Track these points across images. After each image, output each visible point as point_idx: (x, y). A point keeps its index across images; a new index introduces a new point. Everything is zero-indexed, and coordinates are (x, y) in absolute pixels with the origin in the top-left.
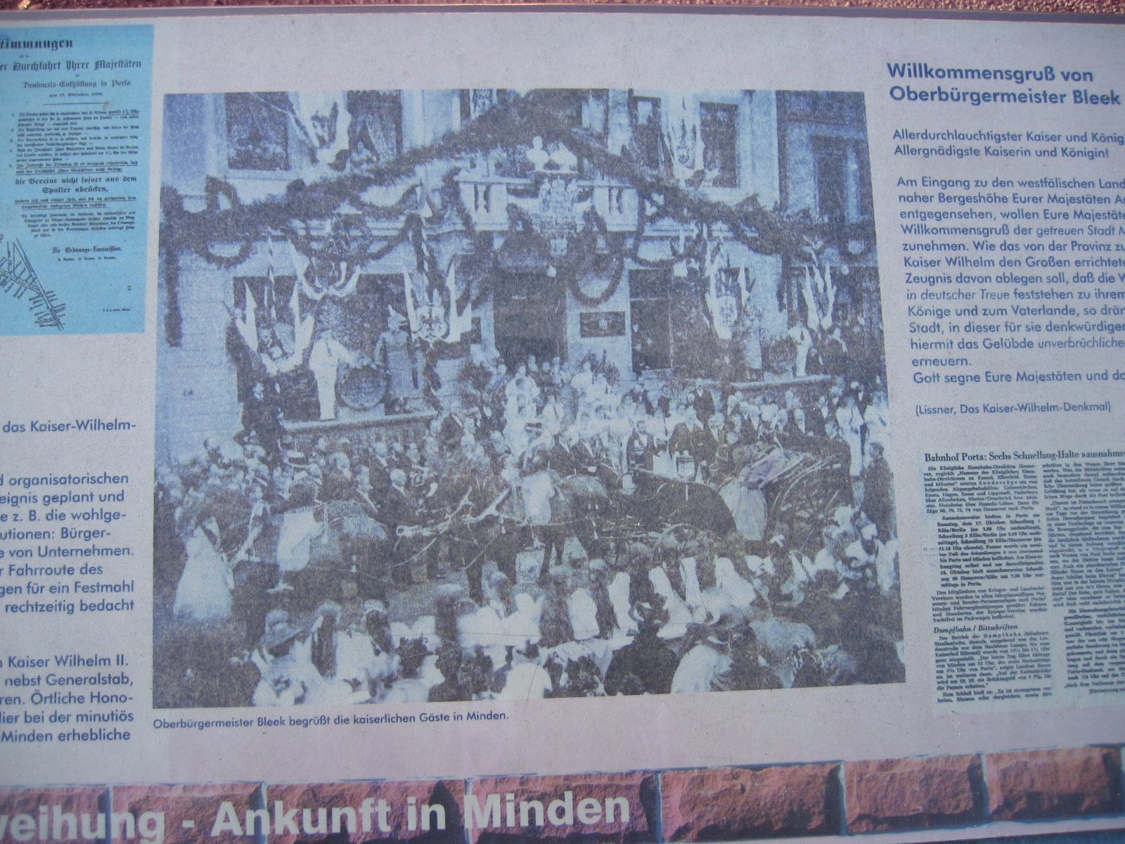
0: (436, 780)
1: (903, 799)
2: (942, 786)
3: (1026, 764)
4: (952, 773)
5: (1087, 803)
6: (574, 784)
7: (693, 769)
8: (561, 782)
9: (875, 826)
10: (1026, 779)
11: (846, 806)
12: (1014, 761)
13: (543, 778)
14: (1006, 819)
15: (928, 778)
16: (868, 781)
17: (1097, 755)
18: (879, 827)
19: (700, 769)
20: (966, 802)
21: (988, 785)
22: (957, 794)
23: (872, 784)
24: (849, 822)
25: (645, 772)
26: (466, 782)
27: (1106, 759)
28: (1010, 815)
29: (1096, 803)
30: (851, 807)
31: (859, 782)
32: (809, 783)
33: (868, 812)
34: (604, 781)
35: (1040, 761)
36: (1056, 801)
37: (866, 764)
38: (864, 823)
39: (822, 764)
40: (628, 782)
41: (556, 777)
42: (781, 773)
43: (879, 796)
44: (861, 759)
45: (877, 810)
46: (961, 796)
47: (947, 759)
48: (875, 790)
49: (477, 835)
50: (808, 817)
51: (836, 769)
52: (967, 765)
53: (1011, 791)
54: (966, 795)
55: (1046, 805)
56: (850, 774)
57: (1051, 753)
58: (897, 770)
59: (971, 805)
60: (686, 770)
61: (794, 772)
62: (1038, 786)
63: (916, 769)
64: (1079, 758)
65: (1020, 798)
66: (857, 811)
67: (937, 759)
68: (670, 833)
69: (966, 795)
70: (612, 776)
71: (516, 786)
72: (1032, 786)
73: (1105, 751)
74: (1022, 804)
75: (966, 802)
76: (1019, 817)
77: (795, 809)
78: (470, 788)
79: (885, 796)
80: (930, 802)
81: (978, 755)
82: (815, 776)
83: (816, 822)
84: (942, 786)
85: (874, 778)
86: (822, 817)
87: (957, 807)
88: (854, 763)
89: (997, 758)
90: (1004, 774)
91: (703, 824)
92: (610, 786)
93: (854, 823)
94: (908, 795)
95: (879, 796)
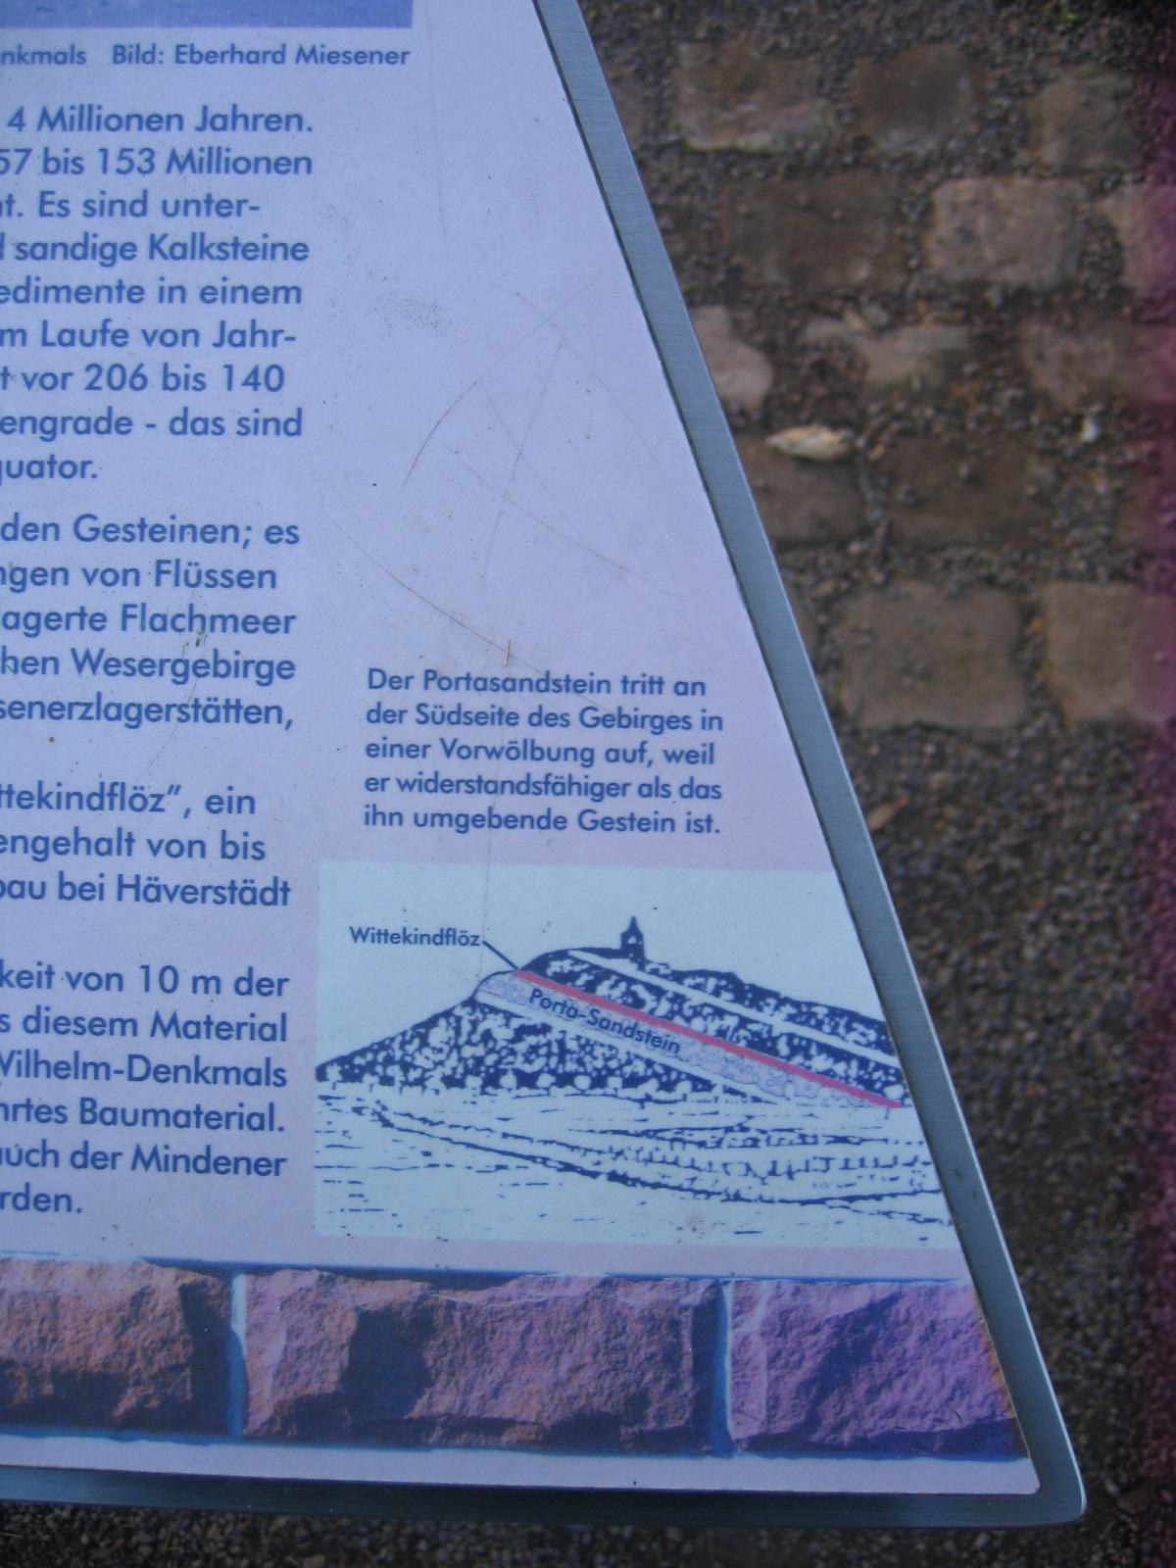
5: (128, 1401)
17: (167, 1286)
27: (189, 1296)
29: (154, 1403)
36: (48, 1388)
55: (22, 1393)
57: (45, 1268)
64: (122, 1288)
73: (190, 1278)
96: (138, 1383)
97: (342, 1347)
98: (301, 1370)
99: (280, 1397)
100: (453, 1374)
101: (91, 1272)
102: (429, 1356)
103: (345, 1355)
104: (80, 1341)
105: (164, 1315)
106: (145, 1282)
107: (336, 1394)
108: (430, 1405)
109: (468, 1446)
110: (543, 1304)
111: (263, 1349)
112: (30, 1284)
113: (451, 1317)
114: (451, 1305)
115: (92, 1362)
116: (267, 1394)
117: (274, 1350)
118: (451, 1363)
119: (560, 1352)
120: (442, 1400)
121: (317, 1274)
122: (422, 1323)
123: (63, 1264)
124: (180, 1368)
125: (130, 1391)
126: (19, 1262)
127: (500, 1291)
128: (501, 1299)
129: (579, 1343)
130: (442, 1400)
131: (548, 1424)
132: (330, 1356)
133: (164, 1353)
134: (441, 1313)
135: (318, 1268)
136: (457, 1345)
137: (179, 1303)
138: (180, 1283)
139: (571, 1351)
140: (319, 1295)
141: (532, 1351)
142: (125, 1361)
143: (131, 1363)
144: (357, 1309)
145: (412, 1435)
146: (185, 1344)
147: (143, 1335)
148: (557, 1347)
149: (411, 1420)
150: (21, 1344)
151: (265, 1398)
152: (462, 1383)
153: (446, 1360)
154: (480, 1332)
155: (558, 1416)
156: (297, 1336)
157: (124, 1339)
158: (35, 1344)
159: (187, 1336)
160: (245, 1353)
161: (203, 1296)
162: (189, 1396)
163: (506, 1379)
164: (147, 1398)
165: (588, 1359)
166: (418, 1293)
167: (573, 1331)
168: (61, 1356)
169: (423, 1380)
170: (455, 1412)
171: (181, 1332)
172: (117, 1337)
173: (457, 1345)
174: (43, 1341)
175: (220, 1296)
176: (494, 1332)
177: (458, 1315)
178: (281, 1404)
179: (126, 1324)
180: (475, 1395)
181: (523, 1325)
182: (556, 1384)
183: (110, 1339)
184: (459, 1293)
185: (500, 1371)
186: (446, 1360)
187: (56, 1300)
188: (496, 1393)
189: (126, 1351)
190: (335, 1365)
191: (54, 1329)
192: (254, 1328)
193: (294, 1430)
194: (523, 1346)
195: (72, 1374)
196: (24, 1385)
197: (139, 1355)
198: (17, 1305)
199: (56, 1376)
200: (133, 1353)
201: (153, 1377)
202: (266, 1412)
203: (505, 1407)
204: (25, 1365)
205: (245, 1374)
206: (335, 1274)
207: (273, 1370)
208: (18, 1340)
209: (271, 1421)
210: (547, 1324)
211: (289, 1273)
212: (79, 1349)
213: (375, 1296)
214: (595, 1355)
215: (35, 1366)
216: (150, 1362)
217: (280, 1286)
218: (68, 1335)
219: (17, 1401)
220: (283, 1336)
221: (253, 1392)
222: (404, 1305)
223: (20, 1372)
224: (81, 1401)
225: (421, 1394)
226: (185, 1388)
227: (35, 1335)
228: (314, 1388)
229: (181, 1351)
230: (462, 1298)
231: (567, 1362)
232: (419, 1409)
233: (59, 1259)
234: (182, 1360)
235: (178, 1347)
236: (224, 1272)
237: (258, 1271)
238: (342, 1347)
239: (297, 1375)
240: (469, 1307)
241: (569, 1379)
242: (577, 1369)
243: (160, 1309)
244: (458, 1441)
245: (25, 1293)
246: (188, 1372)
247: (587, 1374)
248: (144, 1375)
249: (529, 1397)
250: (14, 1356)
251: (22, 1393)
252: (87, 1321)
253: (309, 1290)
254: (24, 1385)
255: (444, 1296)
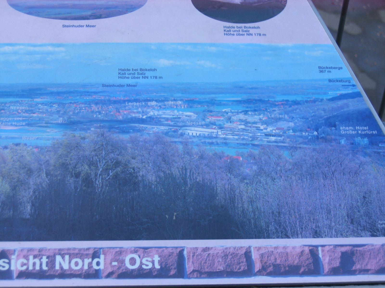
0: (2, 249)
1: (214, 264)
2: (233, 260)
3: (272, 252)
4: (237, 254)
5: (302, 270)
6: (63, 252)
7: (117, 248)
8: (57, 251)
9: (200, 275)
10: (272, 258)
11: (187, 266)
12: (267, 250)
13: (49, 250)
14: (263, 275)
15: (226, 256)
16: (197, 256)
17: (307, 249)
18: (203, 276)
19: (120, 248)
20: (243, 267)
21: (254, 260)
22: (240, 263)
23: (199, 257)
24: (188, 273)
25: (95, 248)
26: (15, 251)
27: (311, 251)
28: (265, 273)
29: (307, 270)
30: (189, 267)
31: (193, 256)
32: (170, 256)
33: (197, 269)
34: (76, 251)
35: (279, 251)
36: (287, 269)
37: (197, 248)
38: (195, 274)
39: (177, 248)
40: (87, 252)
41: (55, 249)
42: (157, 251)
43: (203, 262)
44: (195, 246)
45: (201, 268)
46: (240, 265)
47: (235, 248)
48: (201, 260)
49: (18, 273)
50: (169, 270)
51: (183, 250)
52: (244, 251)
53: (266, 263)
54: (244, 264)
55: (283, 270)
56: (189, 253)
57: (284, 248)
58: (211, 252)
59: (246, 268)
60: (114, 248)
61: (163, 251)
62: (278, 262)
63: (220, 252)
64: (299, 250)
65: (270, 266)
66: (192, 269)
67: (230, 248)
68: (105, 274)
69: (244, 264)
70: (80, 250)
71: (36, 253)
72: (276, 261)
73: (311, 248)
74: (271, 269)
75: (243, 267)
76: (270, 274)
77: (163, 266)
78: (16, 253)
79: (205, 263)
80: (227, 265)
81: (250, 247)
82: (173, 253)
83: (172, 272)
84: (233, 260)
85: (200, 254)
86: (176, 270)
87: (240, 268)
88: (191, 248)
89: (259, 249)
90: (262, 256)
91: (120, 271)
92: (79, 254)
93: (190, 273)
94: (216, 261)
95: (203, 262)
96: (303, 267)
97: (339, 258)
98: (332, 263)
99: (329, 267)
100: (359, 262)
101: (293, 248)
102: (354, 259)
103: (340, 260)
104: (292, 260)
105: (307, 254)
106: (303, 249)
107: (339, 267)
108: (355, 267)
109: (363, 274)
110: (372, 249)
111: (325, 260)
112: (282, 250)
113: (357, 252)
114: (357, 250)
115: (295, 263)
116: (327, 267)
117: (327, 259)
118: (358, 260)
119: (377, 257)
120: (357, 266)
121: (333, 246)
122: (352, 253)
123: (288, 247)
124: (310, 264)
125: (302, 268)
126: (280, 247)
127: (365, 247)
128: (365, 249)
129: (379, 255)
130: (357, 266)
131: (376, 270)
132: (337, 260)
133: (308, 261)
134: (355, 251)
135: (334, 245)
136: (359, 257)
137: (309, 252)
138: (309, 249)
139: (378, 257)
140: (334, 249)
141: (372, 257)
142: (301, 263)
143: (302, 263)
144: (341, 252)
145: (353, 273)
146: (311, 259)
147: (304, 258)
148: (376, 256)
149: (352, 270)
150: (282, 261)
151: (326, 268)
152: (360, 263)
153: (357, 259)
154: (362, 254)
155: (378, 268)
156: (331, 257)
157: (300, 259)
158: (284, 261)
159: (311, 258)
160: (322, 260)
161: (313, 251)
162: (313, 268)
163: (368, 262)
164: (305, 269)
165: (381, 258)
166: (351, 248)
167: (378, 253)
168: (289, 263)
169: (354, 263)
170: (360, 268)
171: (310, 257)
172: (299, 259)
173: (359, 257)
174: (286, 260)
175: (316, 250)
176: (365, 254)
177: (358, 252)
178: (329, 269)
179: (300, 256)
180: (363, 265)
181: (369, 253)
182: (377, 262)
183: (298, 259)
184: (358, 248)
185: (367, 261)
186: (357, 259)
187: (287, 253)
188: (367, 265)
189: (301, 261)
190: (338, 261)
191: (287, 258)
192: (323, 256)
193: (332, 273)
194: (370, 256)
195: (291, 266)
196: (283, 268)
197: (303, 261)
198: (280, 254)
199: (288, 266)
200: (302, 261)
201: (306, 265)
202: (327, 270)
203: (369, 267)
204: (283, 265)
205: (322, 264)
206: (336, 246)
207: (327, 263)
208: (281, 260)
209: (328, 272)
210: (374, 252)
211: (328, 247)
212: (292, 261)
213: (344, 249)
214: (383, 257)
215: (285, 265)
216: (305, 263)
217: (327, 248)
218: (290, 259)
219: (282, 271)
220: (328, 257)
221: (324, 267)
222: (349, 250)
223: (282, 266)
224: (293, 270)
225: (354, 266)
226: (312, 268)
227: (284, 259)
228: (335, 266)
229: (311, 261)
230: (359, 249)
231: (378, 259)
232: (354, 268)
233: (288, 246)
234: (311, 262)
235: (310, 260)
236: (317, 247)
237: (323, 246)
238: (339, 258)
239: (331, 264)
240: (360, 250)
241: (379, 262)
242: (380, 260)
243: (306, 254)
244: (361, 273)
245: (281, 252)
246: (312, 264)
247: (382, 261)
248: (304, 265)
249: (372, 265)
250: (281, 263)
251: (283, 270)
252: (293, 256)
253: (332, 249)
254: (283, 268)
255: (355, 249)
